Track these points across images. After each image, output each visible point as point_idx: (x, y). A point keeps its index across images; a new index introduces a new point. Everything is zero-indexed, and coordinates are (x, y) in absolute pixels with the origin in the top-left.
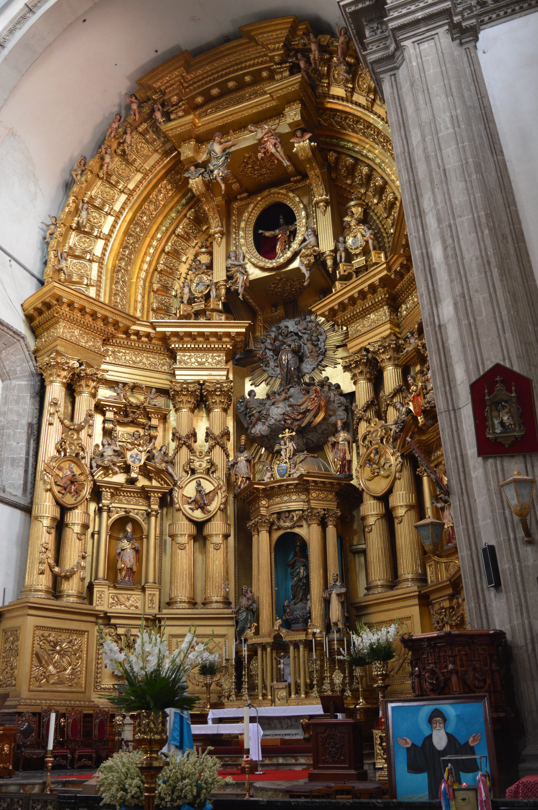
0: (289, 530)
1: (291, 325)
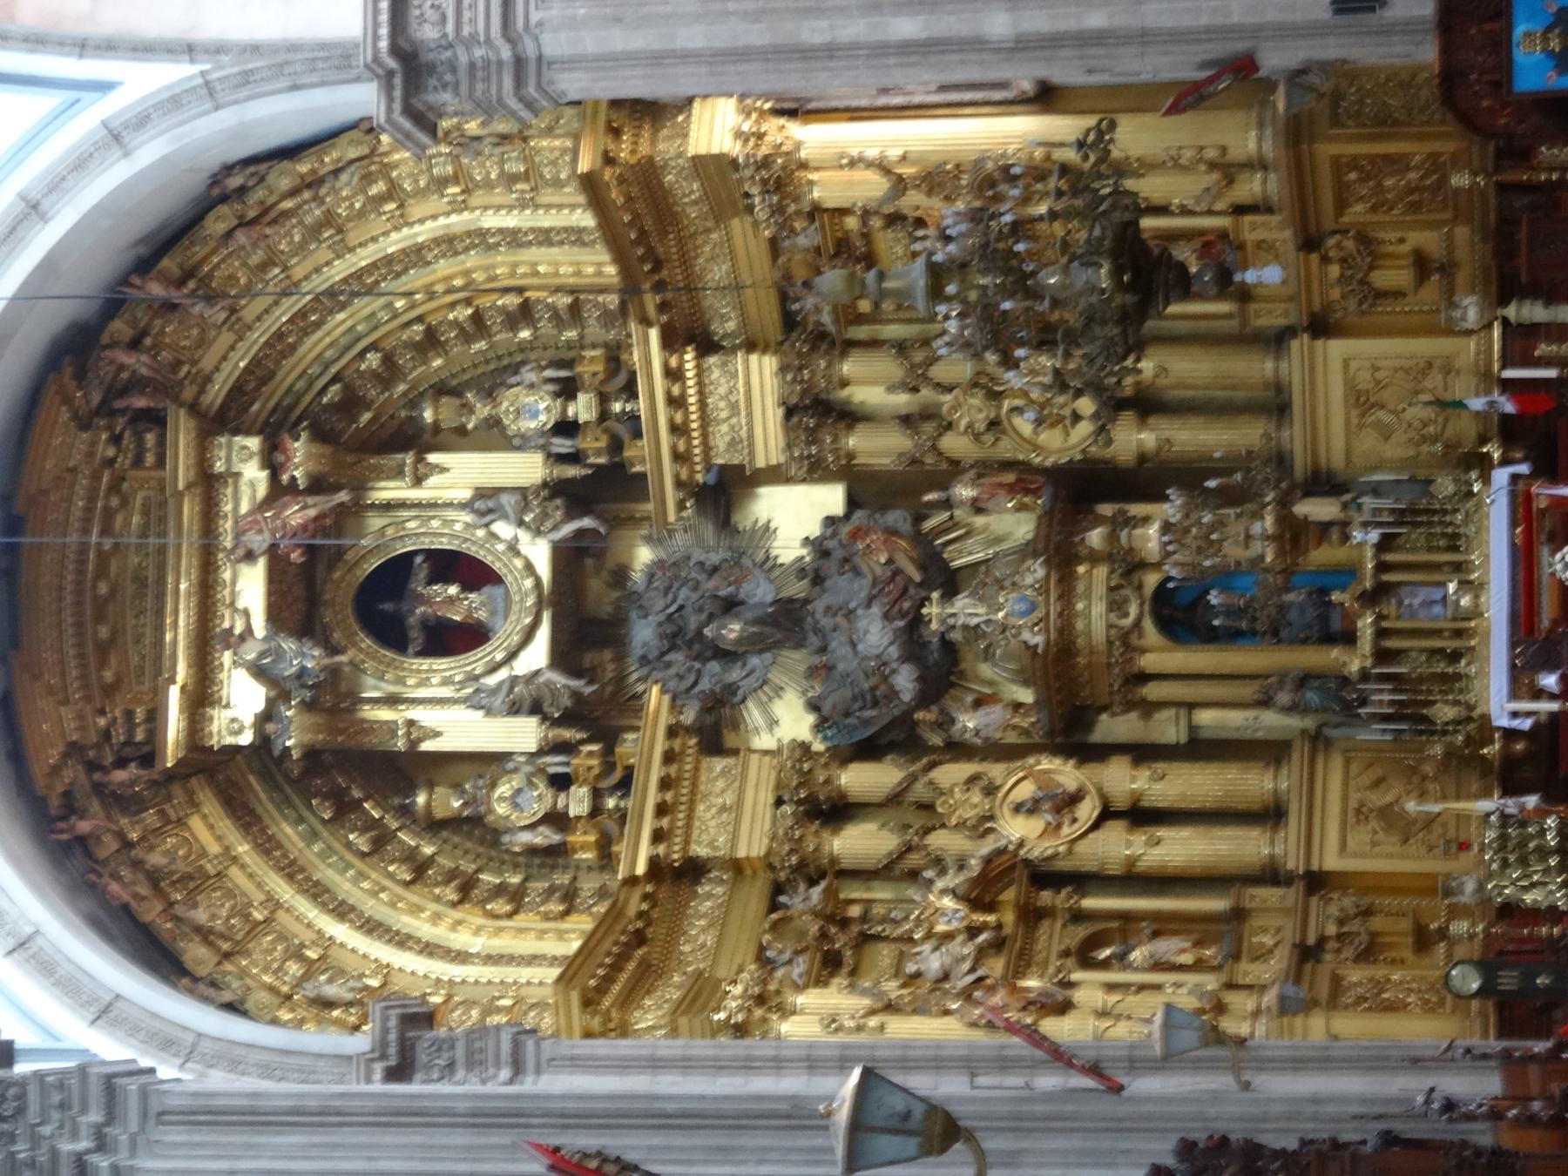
0: (1147, 607)
1: (643, 633)
